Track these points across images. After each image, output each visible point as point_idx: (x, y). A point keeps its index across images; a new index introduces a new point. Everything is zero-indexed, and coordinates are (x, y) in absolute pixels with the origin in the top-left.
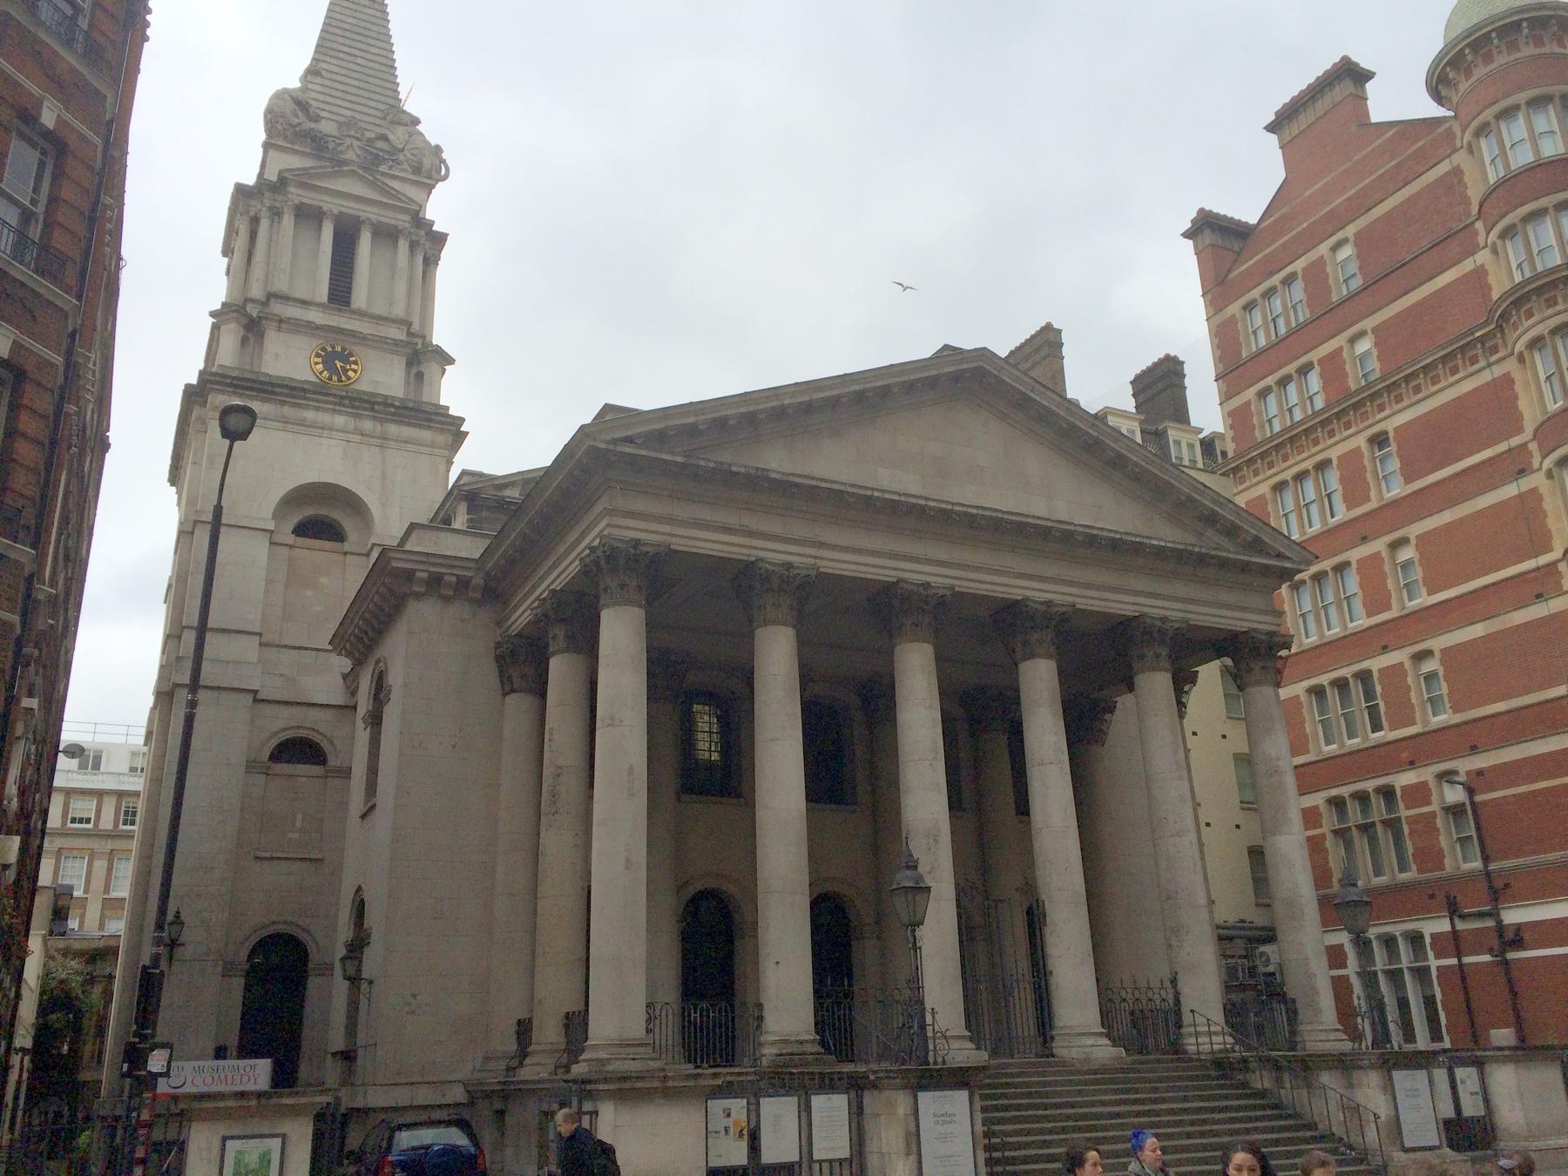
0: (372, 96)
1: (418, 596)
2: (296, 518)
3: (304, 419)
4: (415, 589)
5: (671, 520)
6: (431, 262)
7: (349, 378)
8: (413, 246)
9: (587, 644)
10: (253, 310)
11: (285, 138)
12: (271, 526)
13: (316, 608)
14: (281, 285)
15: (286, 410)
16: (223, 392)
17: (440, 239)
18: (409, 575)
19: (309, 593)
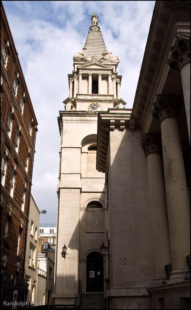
0: (99, 51)
3: (87, 119)
8: (112, 79)
11: (78, 61)
14: (80, 93)
15: (82, 118)
16: (66, 116)
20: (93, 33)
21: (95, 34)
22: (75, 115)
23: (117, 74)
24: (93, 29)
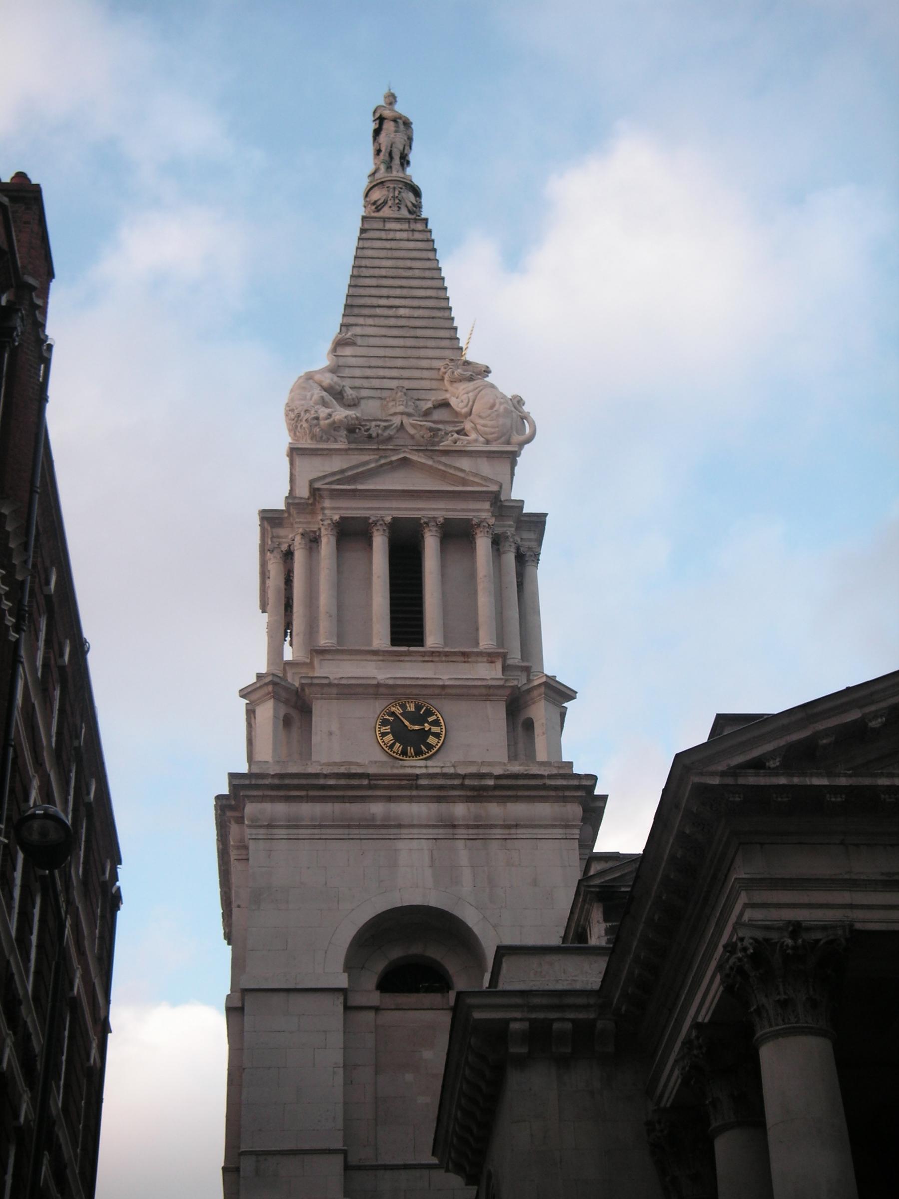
1: (522, 1062)
2: (379, 966)
3: (373, 817)
4: (514, 1049)
5: (852, 884)
6: (526, 559)
7: (430, 747)
8: (497, 542)
9: (751, 1113)
10: (294, 680)
12: (342, 981)
13: (421, 1100)
16: (263, 799)
17: (537, 523)
18: (498, 1033)
19: (409, 1077)
20: (383, 235)
21: (398, 235)
22: (311, 793)
23: (522, 508)
24: (385, 203)
